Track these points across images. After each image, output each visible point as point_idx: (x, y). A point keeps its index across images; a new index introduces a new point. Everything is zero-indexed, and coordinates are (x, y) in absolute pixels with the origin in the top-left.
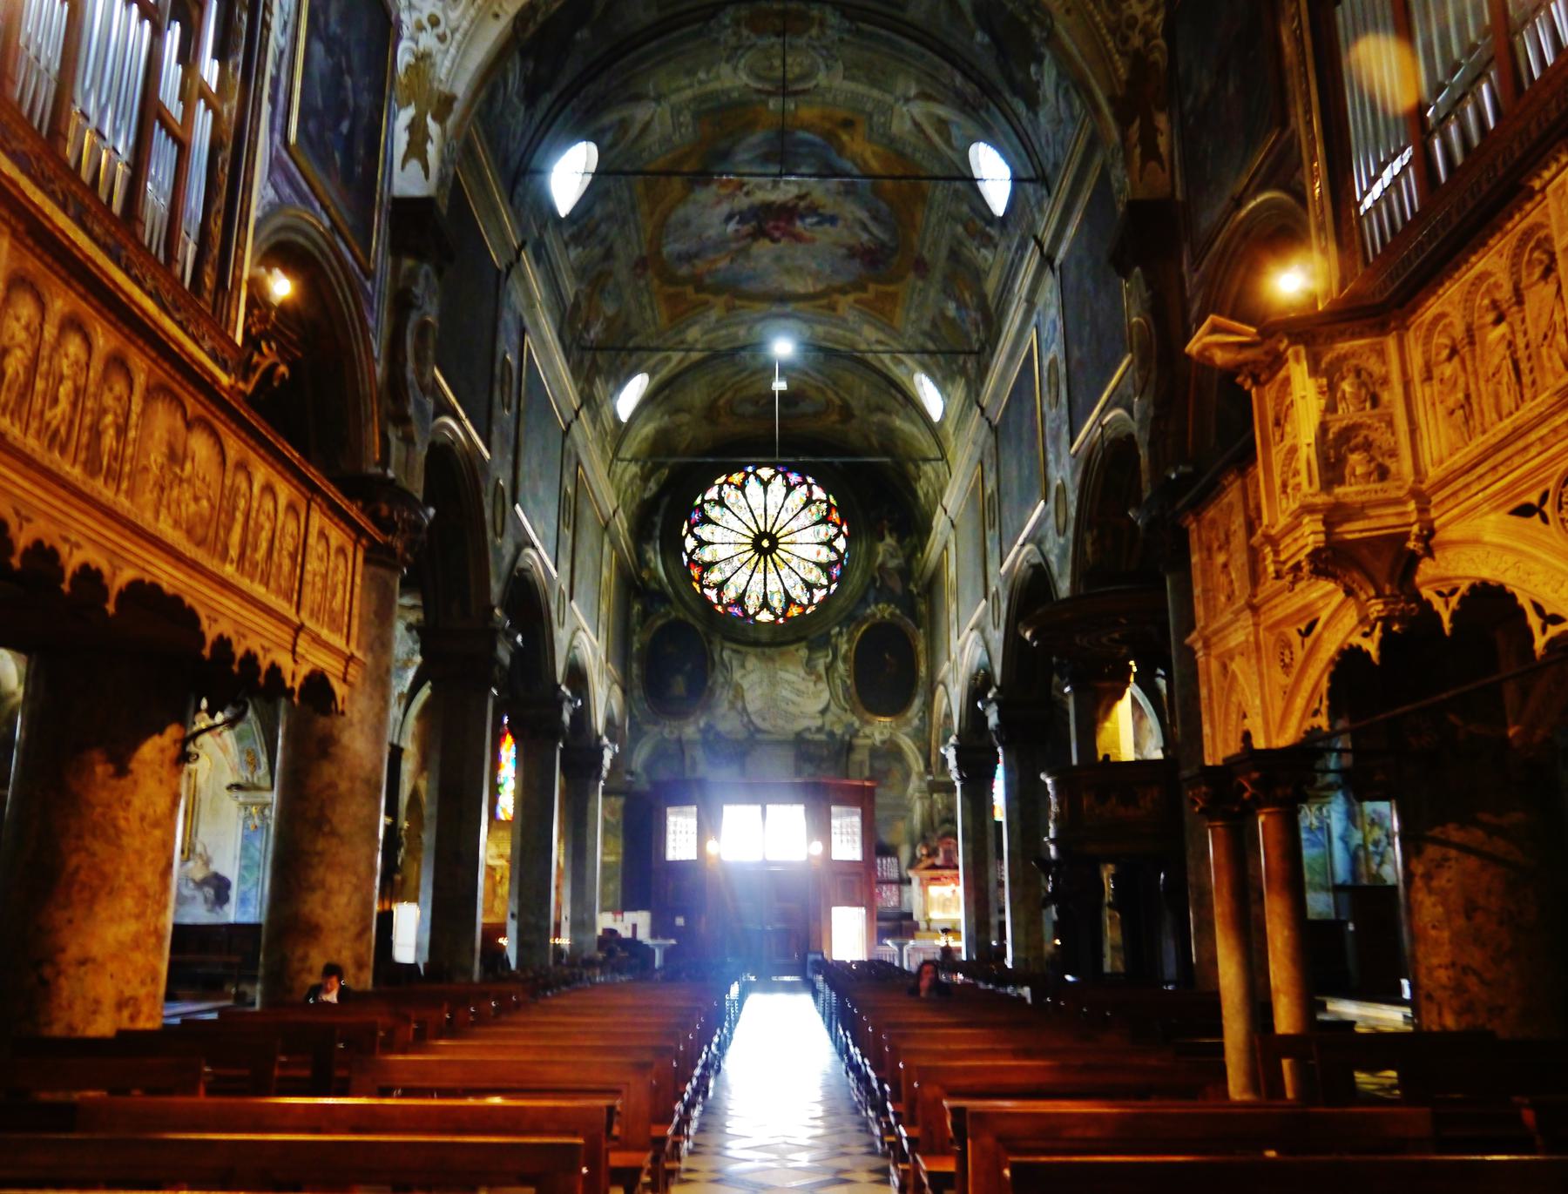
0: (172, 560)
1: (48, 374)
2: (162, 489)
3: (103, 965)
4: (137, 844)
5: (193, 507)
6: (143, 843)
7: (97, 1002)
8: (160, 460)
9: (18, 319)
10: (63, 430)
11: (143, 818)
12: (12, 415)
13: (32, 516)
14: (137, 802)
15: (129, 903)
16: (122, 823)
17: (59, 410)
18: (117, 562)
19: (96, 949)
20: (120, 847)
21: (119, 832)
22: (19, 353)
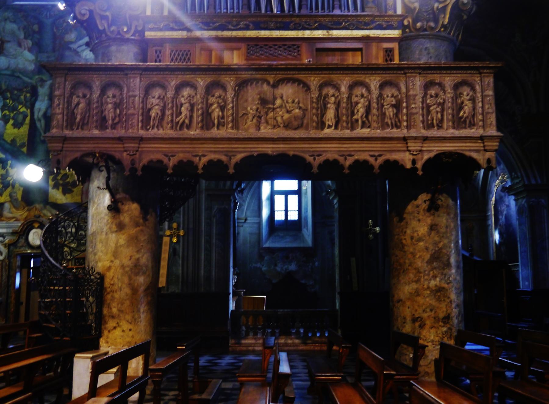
0: (272, 142)
1: (172, 107)
2: (260, 117)
3: (404, 302)
4: (411, 250)
5: (286, 116)
6: (414, 249)
7: (405, 318)
8: (254, 107)
9: (154, 97)
10: (187, 121)
11: (412, 238)
12: (157, 127)
13: (174, 154)
14: (409, 231)
15: (411, 275)
16: (404, 241)
17: (183, 116)
18: (230, 154)
19: (402, 296)
20: (405, 252)
21: (403, 246)
22: (157, 107)
